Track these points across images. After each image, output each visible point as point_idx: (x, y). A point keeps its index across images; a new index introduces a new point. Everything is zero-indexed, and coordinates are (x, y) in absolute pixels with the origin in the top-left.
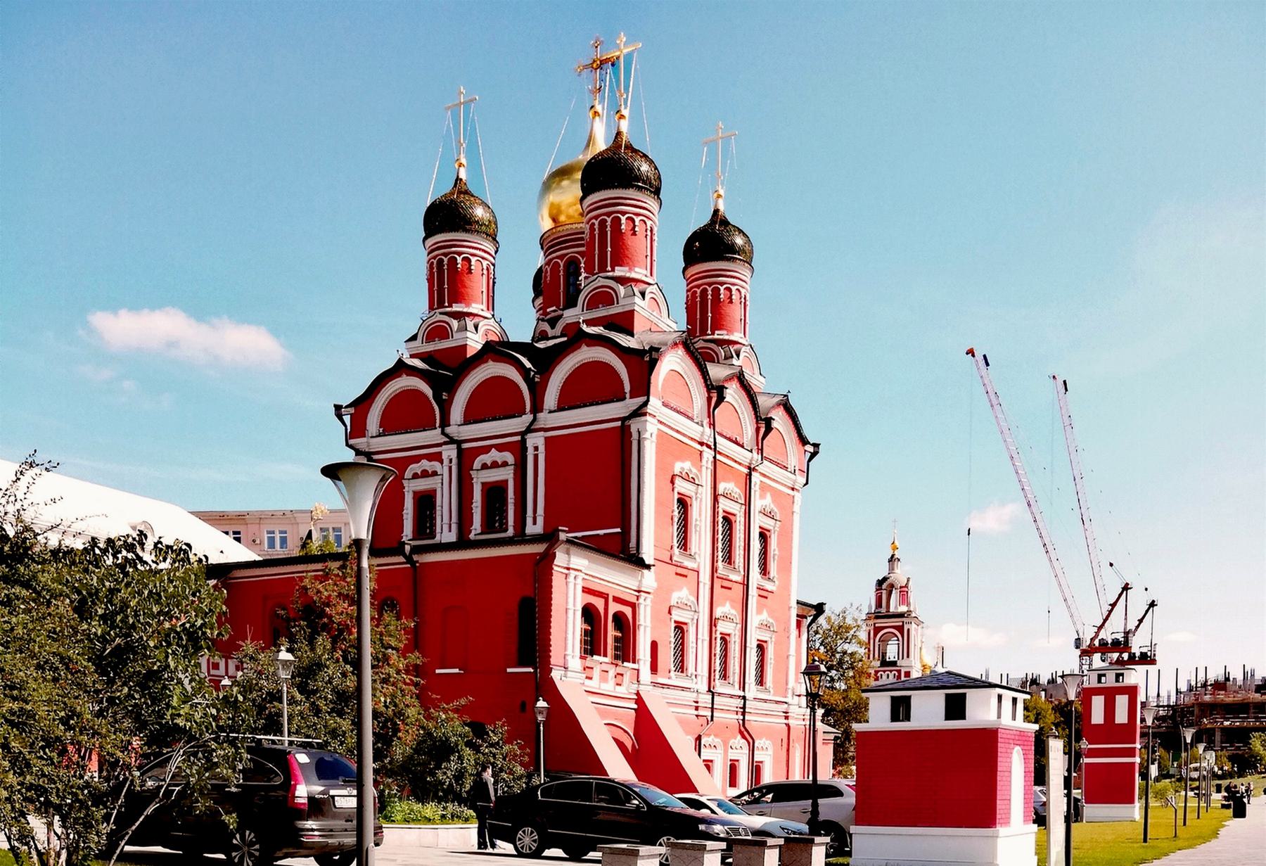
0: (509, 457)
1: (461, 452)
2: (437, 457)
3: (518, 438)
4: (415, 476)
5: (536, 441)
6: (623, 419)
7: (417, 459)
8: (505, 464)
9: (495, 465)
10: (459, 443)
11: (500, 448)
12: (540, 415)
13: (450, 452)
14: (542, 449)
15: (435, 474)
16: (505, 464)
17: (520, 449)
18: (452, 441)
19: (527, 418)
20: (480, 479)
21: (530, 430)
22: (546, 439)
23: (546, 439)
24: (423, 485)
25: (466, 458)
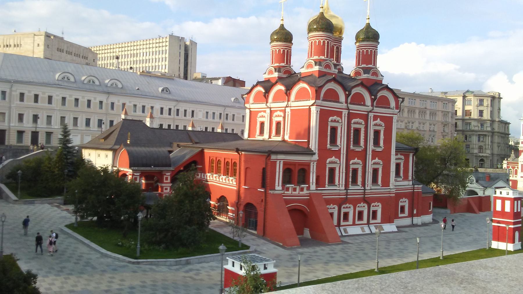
0: (282, 114)
1: (271, 111)
2: (265, 112)
3: (284, 109)
4: (260, 117)
5: (288, 110)
6: (310, 106)
7: (260, 112)
8: (281, 116)
9: (279, 116)
10: (270, 108)
11: (281, 111)
12: (289, 103)
13: (268, 111)
14: (290, 113)
15: (264, 117)
16: (281, 116)
17: (284, 112)
18: (268, 108)
19: (286, 103)
20: (275, 119)
21: (287, 107)
22: (291, 110)
23: (291, 110)
24: (262, 119)
25: (271, 112)
